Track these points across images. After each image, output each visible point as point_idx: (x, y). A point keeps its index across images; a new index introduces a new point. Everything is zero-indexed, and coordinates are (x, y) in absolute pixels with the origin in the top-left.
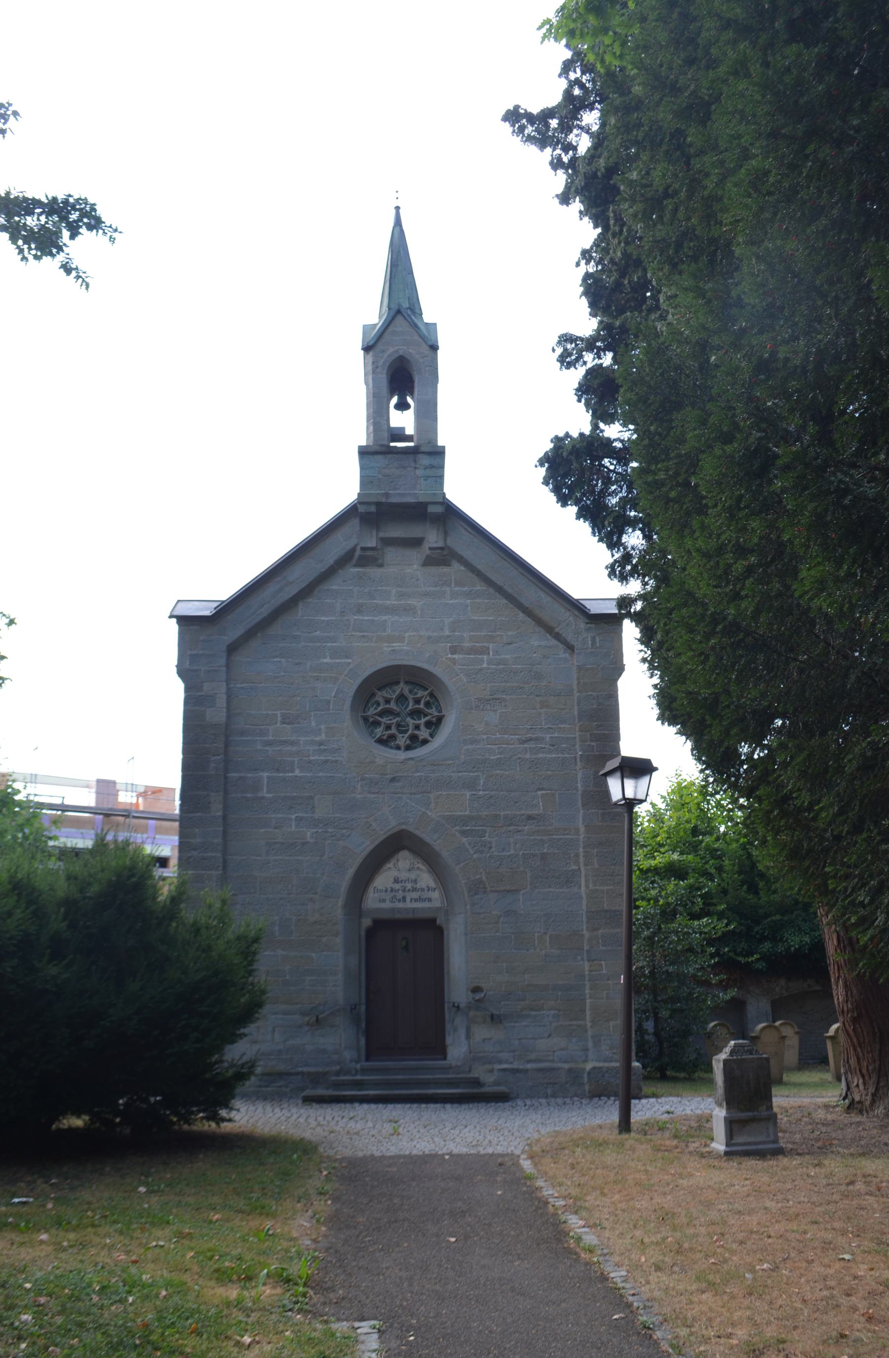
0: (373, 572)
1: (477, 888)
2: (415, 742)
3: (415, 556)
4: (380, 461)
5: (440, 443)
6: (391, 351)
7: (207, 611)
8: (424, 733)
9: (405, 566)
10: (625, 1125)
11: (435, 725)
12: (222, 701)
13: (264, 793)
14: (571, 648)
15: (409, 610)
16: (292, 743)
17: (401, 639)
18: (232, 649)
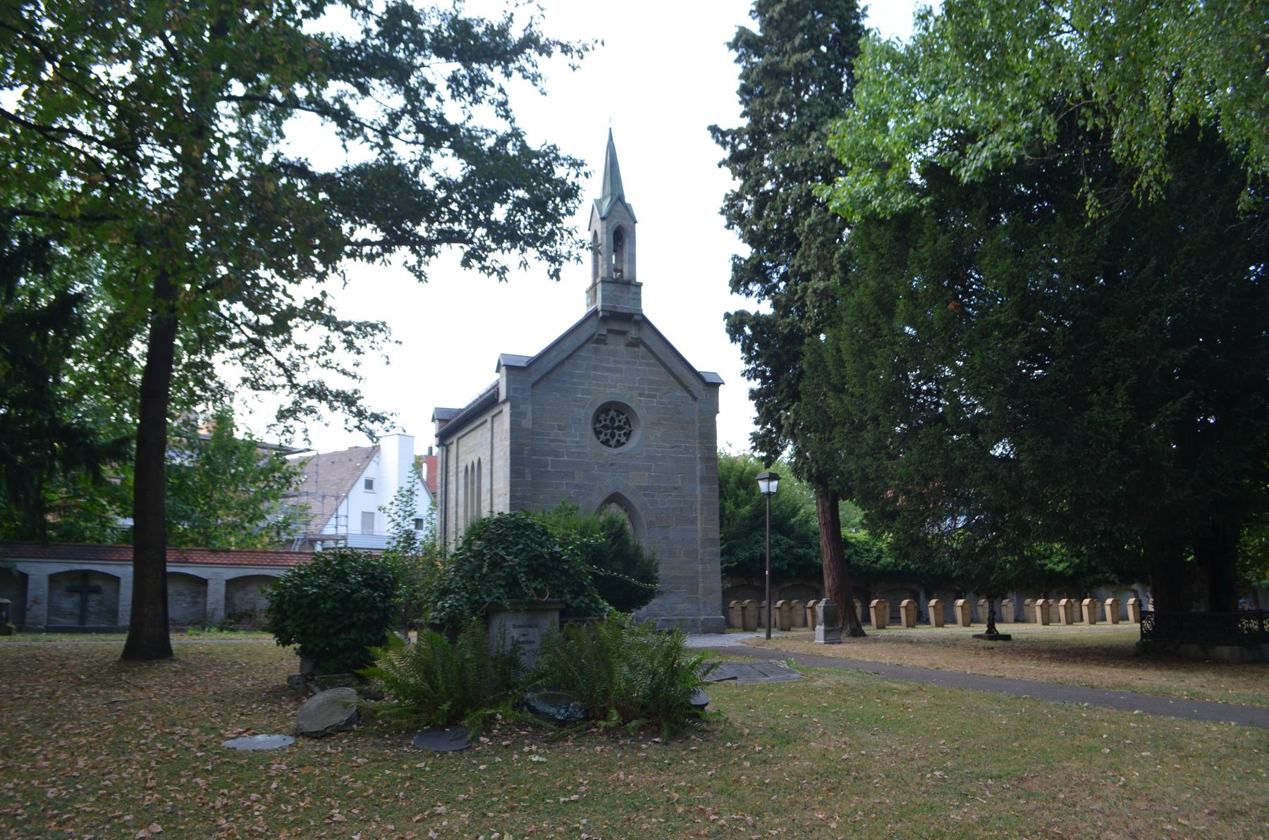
0: (602, 347)
1: (651, 524)
2: (619, 444)
3: (622, 340)
4: (611, 287)
5: (638, 280)
6: (615, 222)
7: (523, 364)
8: (623, 439)
9: (617, 345)
10: (769, 637)
11: (628, 435)
12: (530, 416)
13: (550, 469)
14: (695, 398)
15: (619, 371)
16: (564, 441)
17: (615, 387)
18: (533, 385)
